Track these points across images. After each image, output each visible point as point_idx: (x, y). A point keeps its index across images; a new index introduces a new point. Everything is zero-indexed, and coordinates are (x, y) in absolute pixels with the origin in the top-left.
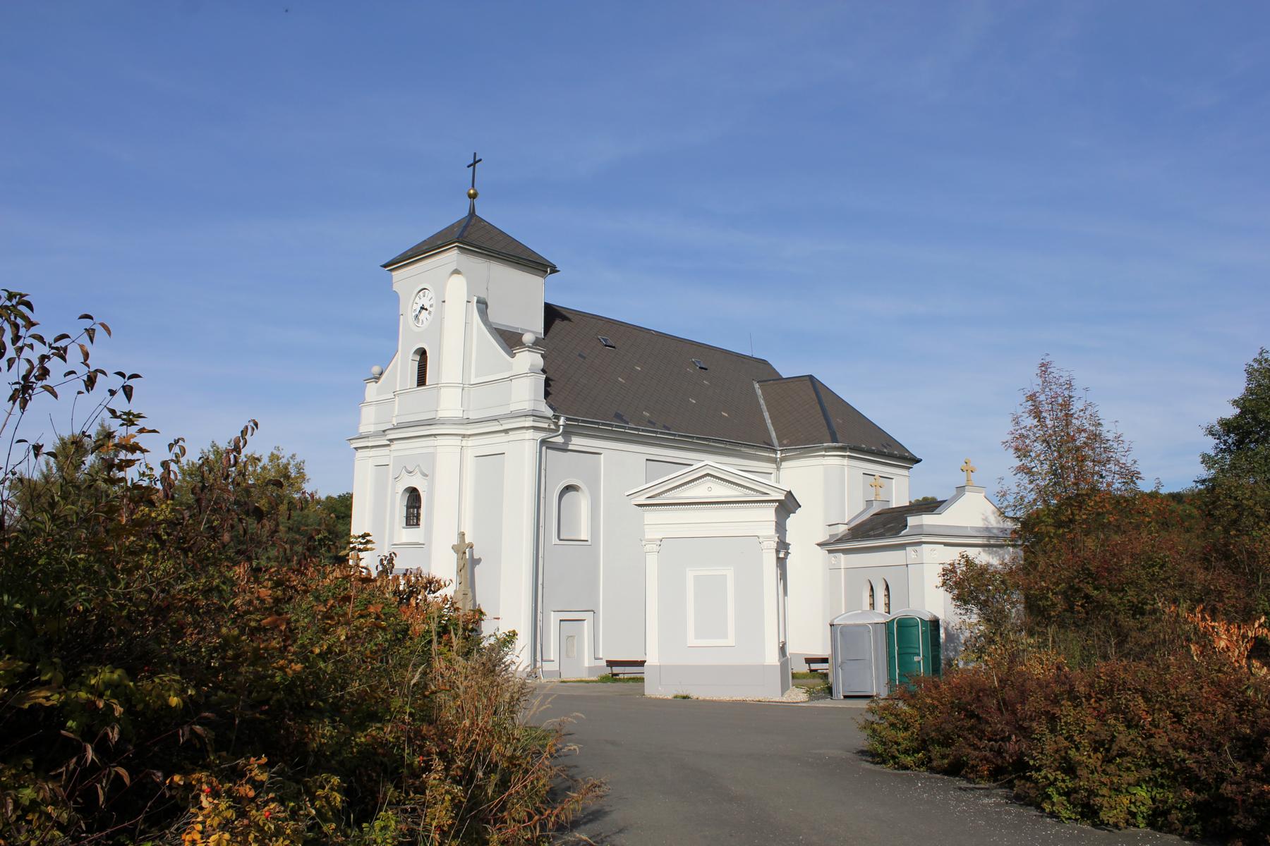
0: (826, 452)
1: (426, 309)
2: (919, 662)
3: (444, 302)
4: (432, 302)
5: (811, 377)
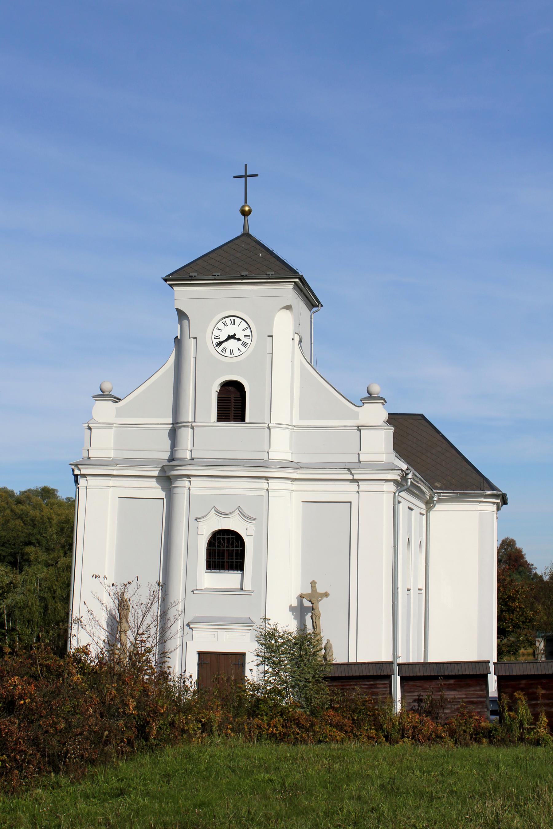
0: (484, 498)
1: (239, 340)
3: (293, 339)
4: (248, 332)
5: (422, 416)
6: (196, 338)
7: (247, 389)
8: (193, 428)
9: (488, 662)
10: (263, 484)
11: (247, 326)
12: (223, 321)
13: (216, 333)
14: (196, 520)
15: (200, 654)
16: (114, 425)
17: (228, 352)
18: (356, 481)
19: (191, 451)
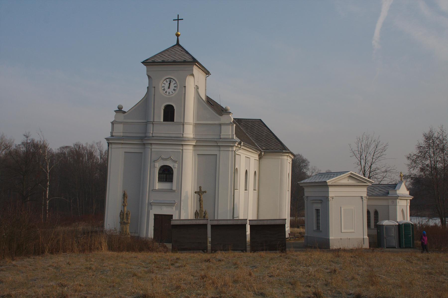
2: (410, 237)
5: (260, 120)
6: (154, 87)
7: (175, 108)
8: (153, 124)
9: (247, 220)
11: (175, 82)
12: (166, 80)
13: (163, 85)
14: (154, 161)
15: (155, 215)
16: (123, 123)
17: (168, 93)
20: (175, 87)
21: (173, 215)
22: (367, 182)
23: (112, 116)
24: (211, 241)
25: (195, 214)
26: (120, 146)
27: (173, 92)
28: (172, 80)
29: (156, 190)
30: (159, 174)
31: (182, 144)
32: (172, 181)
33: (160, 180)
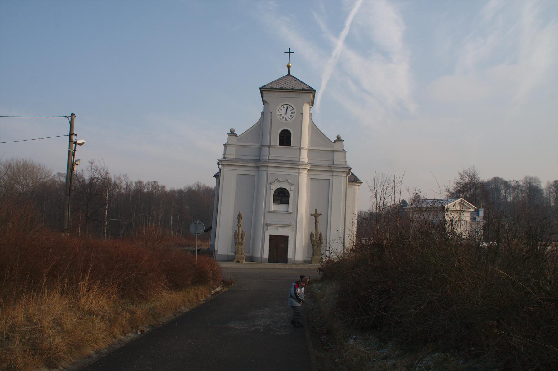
6: (271, 112)
7: (292, 133)
8: (269, 147)
10: (297, 171)
13: (280, 111)
15: (271, 236)
17: (284, 118)
18: (332, 172)
19: (269, 156)
20: (292, 113)
21: (288, 237)
22: (470, 208)
23: (225, 139)
24: (268, 257)
25: (311, 236)
26: (233, 168)
27: (290, 118)
28: (289, 106)
29: (271, 211)
30: (274, 196)
31: (299, 168)
32: (288, 204)
33: (275, 201)
